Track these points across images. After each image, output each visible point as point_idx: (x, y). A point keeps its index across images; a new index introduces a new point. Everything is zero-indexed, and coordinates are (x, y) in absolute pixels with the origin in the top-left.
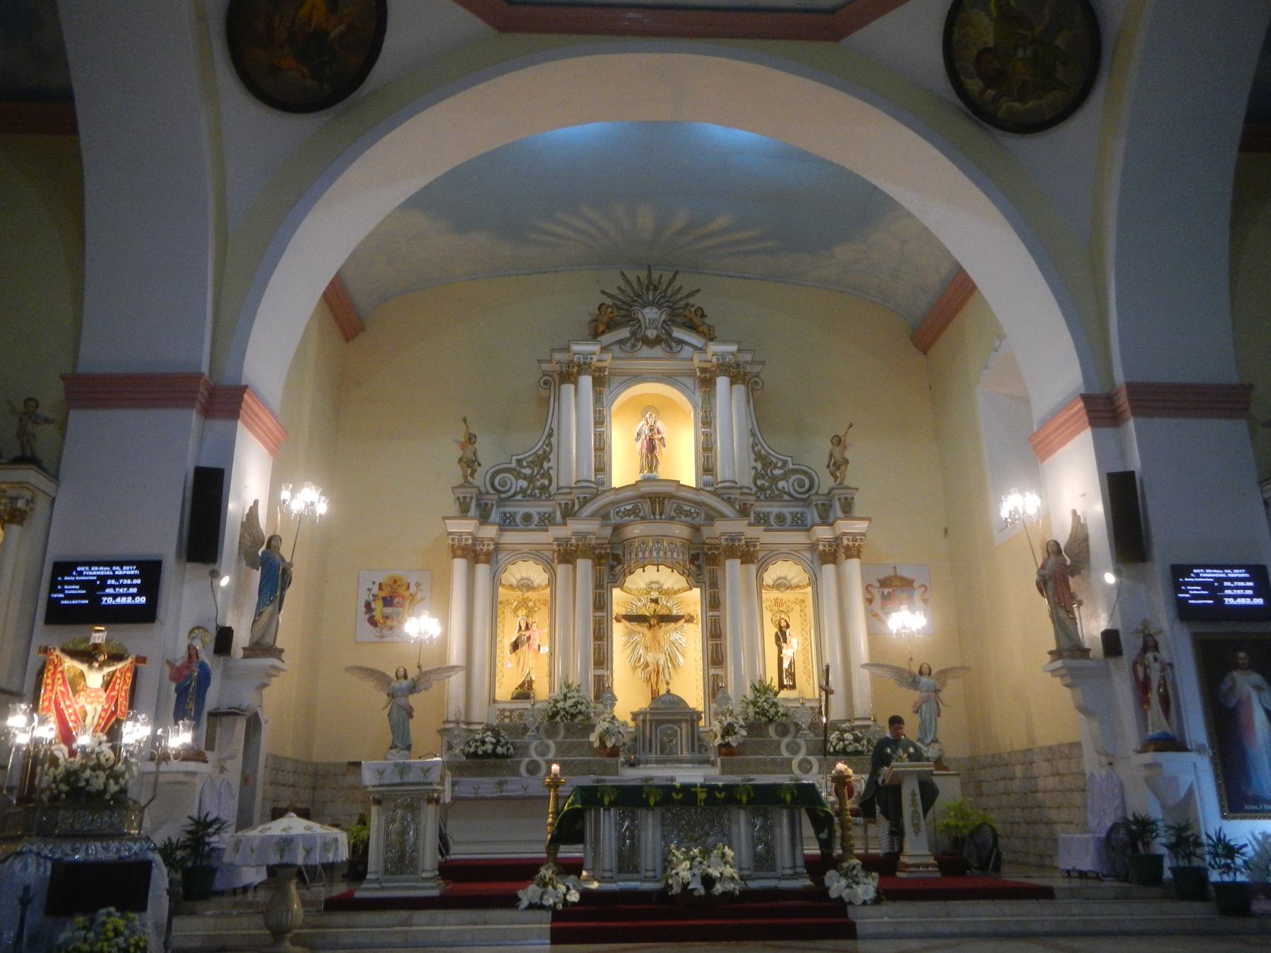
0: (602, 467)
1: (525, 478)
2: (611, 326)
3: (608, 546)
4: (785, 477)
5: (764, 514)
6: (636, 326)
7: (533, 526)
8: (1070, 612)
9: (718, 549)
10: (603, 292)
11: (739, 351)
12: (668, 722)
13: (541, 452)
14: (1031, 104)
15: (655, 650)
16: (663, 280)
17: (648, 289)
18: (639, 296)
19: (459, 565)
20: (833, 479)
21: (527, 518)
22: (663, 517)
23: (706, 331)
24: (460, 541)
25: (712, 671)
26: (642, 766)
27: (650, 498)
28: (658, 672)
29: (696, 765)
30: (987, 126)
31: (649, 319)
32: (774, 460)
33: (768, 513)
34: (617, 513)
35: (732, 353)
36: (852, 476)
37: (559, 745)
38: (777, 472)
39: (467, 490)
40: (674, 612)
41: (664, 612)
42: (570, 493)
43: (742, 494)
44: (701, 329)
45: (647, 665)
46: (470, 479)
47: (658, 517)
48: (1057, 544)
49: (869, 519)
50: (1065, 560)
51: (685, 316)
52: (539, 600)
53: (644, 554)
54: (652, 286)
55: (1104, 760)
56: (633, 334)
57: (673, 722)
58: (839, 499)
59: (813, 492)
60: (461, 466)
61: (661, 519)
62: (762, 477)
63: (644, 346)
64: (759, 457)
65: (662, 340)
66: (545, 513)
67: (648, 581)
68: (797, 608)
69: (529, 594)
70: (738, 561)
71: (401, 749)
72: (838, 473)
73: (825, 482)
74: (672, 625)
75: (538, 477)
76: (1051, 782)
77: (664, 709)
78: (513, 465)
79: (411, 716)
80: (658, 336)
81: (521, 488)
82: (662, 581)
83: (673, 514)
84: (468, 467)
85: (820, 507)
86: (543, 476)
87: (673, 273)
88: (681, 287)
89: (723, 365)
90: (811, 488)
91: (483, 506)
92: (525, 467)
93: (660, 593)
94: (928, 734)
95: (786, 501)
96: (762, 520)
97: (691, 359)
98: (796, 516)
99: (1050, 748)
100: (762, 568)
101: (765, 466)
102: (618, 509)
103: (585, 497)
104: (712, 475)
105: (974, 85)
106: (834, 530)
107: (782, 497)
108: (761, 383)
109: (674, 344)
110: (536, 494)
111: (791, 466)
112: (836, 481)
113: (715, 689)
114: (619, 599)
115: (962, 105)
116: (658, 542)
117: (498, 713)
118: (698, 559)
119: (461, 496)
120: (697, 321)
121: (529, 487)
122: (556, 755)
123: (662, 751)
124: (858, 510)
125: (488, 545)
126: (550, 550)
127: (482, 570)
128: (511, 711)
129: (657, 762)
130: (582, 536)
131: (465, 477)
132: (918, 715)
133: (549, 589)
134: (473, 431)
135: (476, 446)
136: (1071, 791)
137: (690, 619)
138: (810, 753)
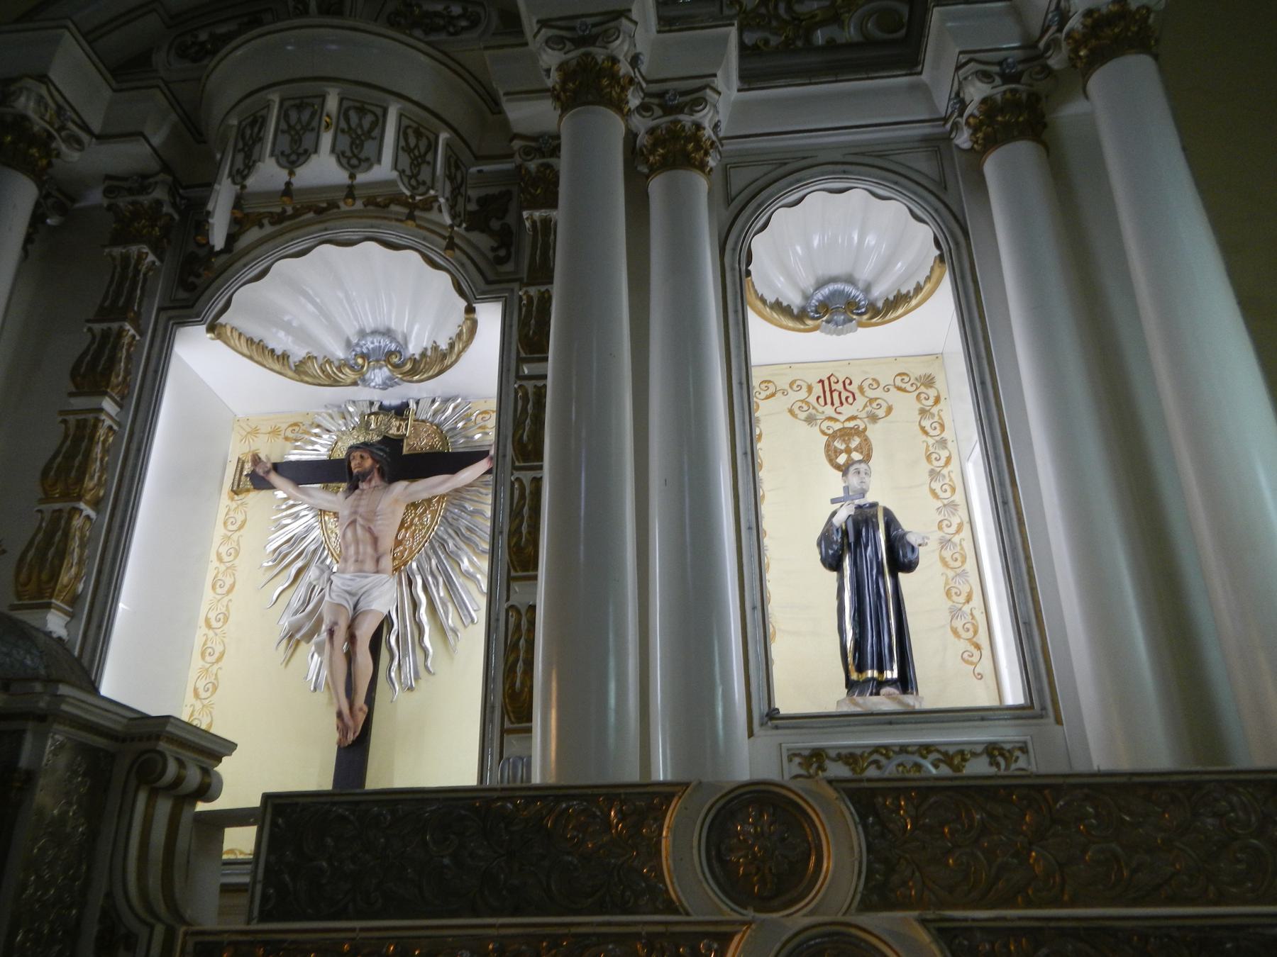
15: (356, 561)
28: (352, 639)
40: (458, 445)
41: (418, 441)
53: (248, 156)
67: (351, 331)
68: (906, 406)
116: (300, 108)
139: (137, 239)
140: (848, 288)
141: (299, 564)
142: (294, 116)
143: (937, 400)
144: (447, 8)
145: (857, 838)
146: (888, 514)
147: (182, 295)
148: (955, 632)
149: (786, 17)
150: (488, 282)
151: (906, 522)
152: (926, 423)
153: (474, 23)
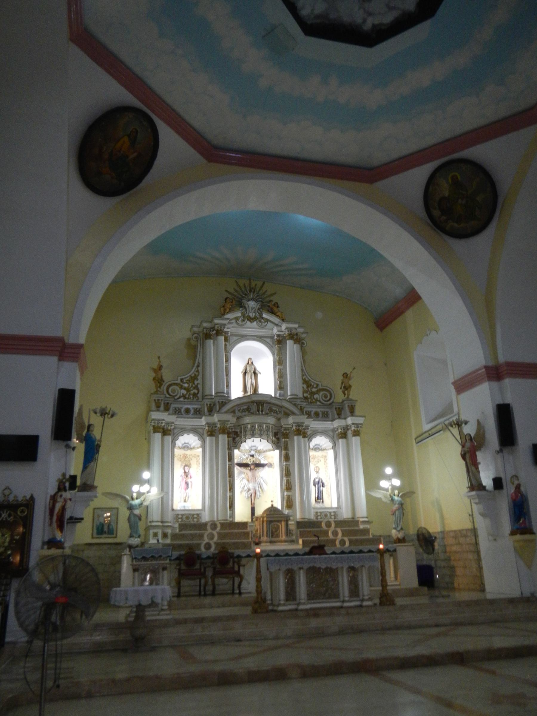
0: (228, 386)
1: (185, 389)
2: (231, 310)
3: (233, 427)
4: (317, 392)
5: (308, 412)
6: (245, 309)
7: (190, 415)
8: (477, 468)
9: (289, 430)
10: (227, 291)
11: (299, 327)
12: (275, 521)
13: (193, 375)
15: (254, 482)
16: (257, 286)
17: (250, 291)
18: (246, 294)
19: (158, 436)
20: (343, 395)
21: (187, 411)
22: (263, 413)
23: (280, 316)
24: (158, 423)
25: (286, 493)
26: (262, 544)
27: (257, 403)
29: (290, 543)
30: (439, 232)
31: (251, 308)
32: (312, 384)
33: (311, 411)
34: (239, 410)
35: (295, 328)
36: (353, 394)
37: (219, 534)
38: (314, 390)
39: (158, 396)
40: (263, 462)
42: (211, 399)
43: (301, 402)
44: (278, 314)
45: (249, 490)
46: (159, 389)
47: (260, 413)
48: (470, 435)
49: (365, 417)
50: (474, 443)
51: (269, 306)
52: (192, 455)
53: (253, 432)
54: (252, 290)
55: (491, 538)
57: (278, 521)
58: (348, 406)
59: (331, 401)
60: (155, 383)
61: (262, 414)
62: (307, 392)
63: (248, 322)
64: (305, 382)
65: (258, 318)
66: (197, 409)
67: (250, 445)
69: (188, 452)
70: (301, 436)
71: (136, 538)
72: (346, 392)
73: (339, 397)
74: (261, 469)
75: (192, 389)
76: (454, 548)
77: (272, 515)
78: (179, 381)
79: (140, 519)
80: (255, 316)
81: (183, 394)
82: (257, 445)
83: (267, 411)
84: (159, 383)
85: (337, 409)
86: (194, 388)
87: (262, 283)
88: (266, 291)
89: (291, 334)
91: (166, 404)
92: (185, 383)
93: (256, 452)
94: (399, 525)
95: (318, 405)
96: (309, 415)
97: (272, 329)
98: (324, 413)
99: (455, 531)
100: (310, 440)
101: (308, 387)
102: (239, 408)
103: (222, 402)
104: (283, 390)
106: (346, 422)
107: (316, 403)
108: (306, 344)
109: (263, 321)
110: (191, 398)
111: (320, 387)
112: (345, 396)
114: (238, 455)
115: (431, 223)
117: (175, 516)
118: (277, 435)
119: (157, 399)
120: (275, 309)
121: (187, 394)
122: (217, 540)
123: (272, 536)
124: (357, 411)
125: (171, 426)
126: (201, 428)
127: (168, 438)
128: (182, 515)
129: (271, 542)
130: (223, 422)
131: (157, 388)
132: (394, 516)
133: (200, 449)
134: (161, 364)
135: (163, 370)
136: (467, 552)
137: (270, 465)
138: (343, 535)
139: (230, 437)
140: (319, 447)
141: (242, 479)
142: (260, 428)
143: (327, 460)
144: (276, 409)
145: (334, 524)
146: (322, 479)
147: (234, 444)
148: (327, 493)
149: (310, 391)
150: (277, 447)
151: (324, 481)
152: (325, 463)
153: (280, 412)
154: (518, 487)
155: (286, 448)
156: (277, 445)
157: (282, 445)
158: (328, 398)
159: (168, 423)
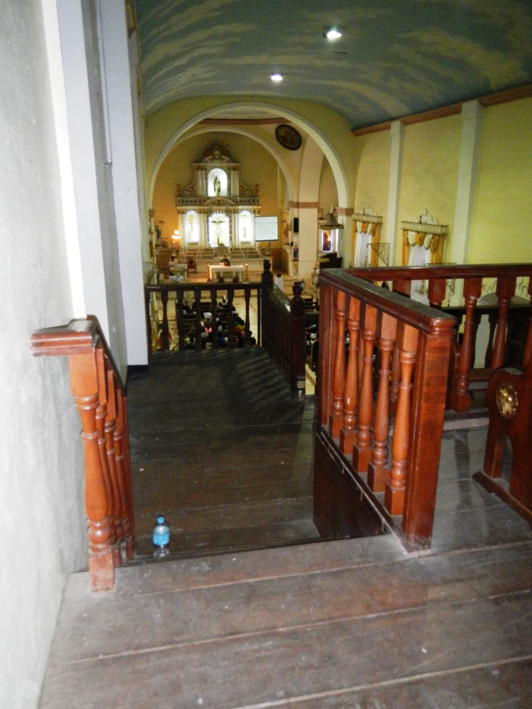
0: (207, 190)
2: (208, 155)
4: (246, 190)
14: (291, 146)
21: (191, 201)
36: (260, 193)
41: (220, 221)
56: (213, 157)
74: (221, 223)
90: (252, 193)
105: (281, 140)
111: (248, 188)
113: (231, 239)
114: (211, 219)
130: (205, 209)
137: (225, 222)
154: (296, 246)
155: (230, 217)
156: (227, 215)
157: (229, 216)
158: (251, 193)
159: (183, 209)
